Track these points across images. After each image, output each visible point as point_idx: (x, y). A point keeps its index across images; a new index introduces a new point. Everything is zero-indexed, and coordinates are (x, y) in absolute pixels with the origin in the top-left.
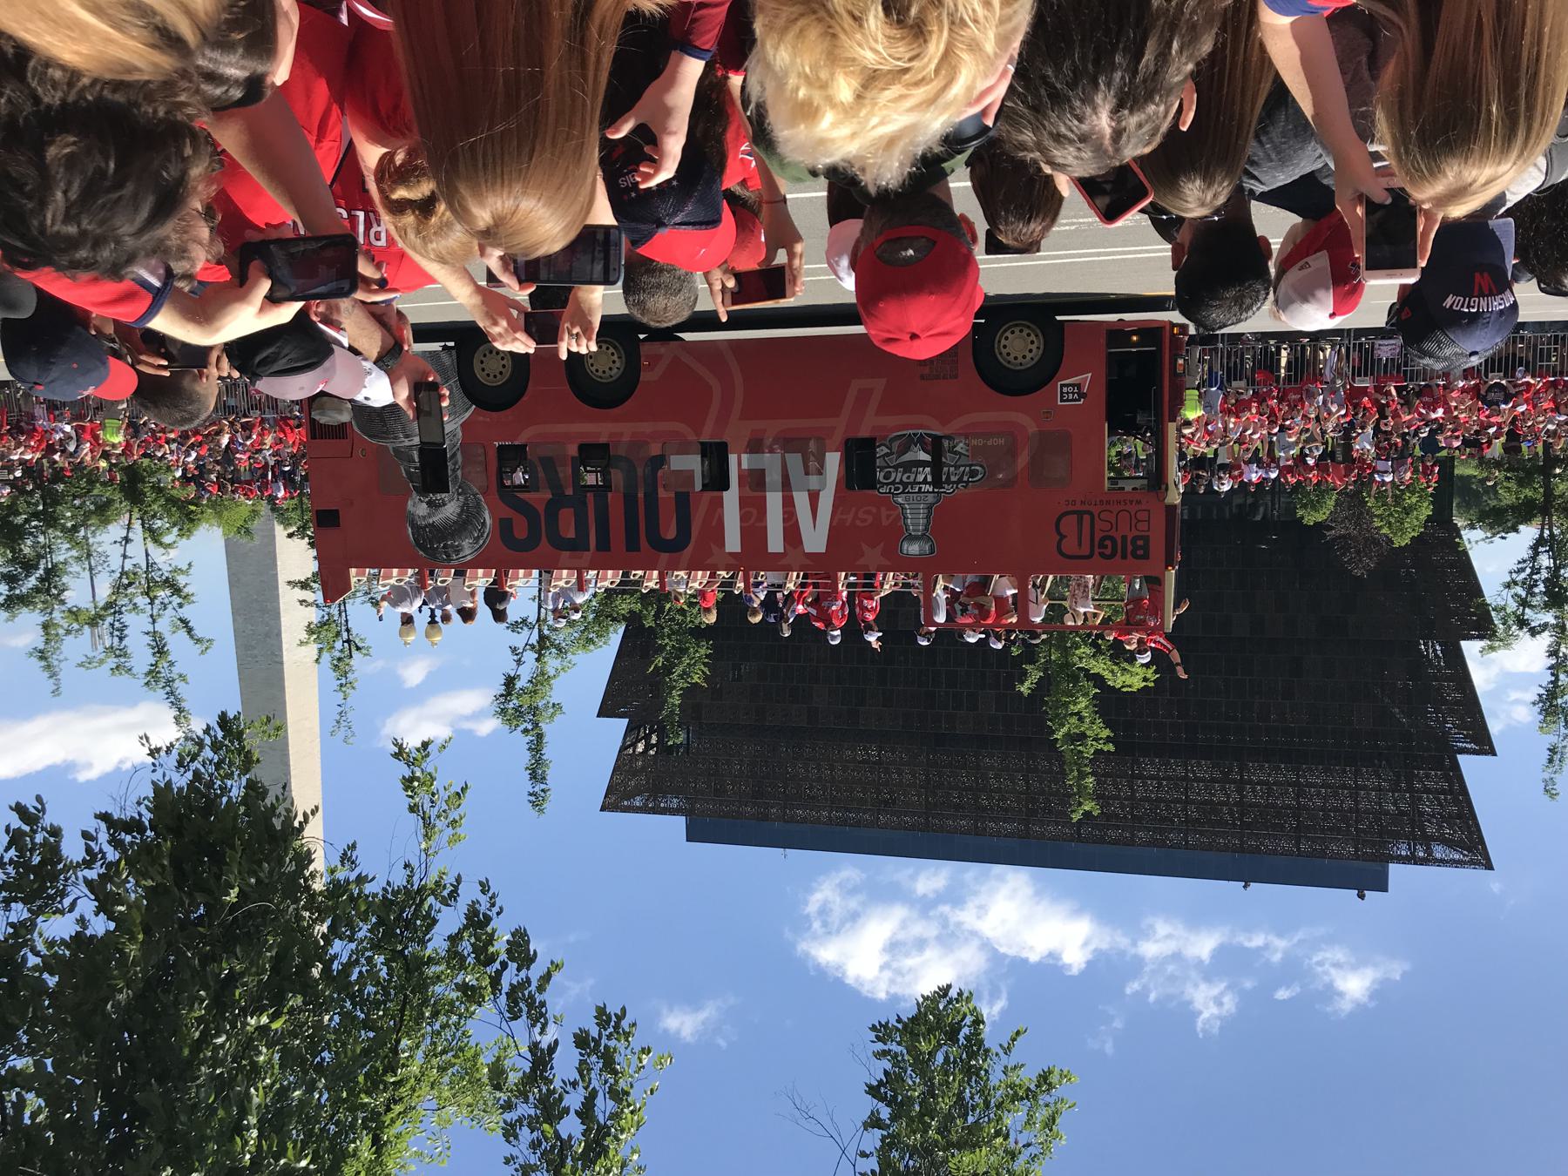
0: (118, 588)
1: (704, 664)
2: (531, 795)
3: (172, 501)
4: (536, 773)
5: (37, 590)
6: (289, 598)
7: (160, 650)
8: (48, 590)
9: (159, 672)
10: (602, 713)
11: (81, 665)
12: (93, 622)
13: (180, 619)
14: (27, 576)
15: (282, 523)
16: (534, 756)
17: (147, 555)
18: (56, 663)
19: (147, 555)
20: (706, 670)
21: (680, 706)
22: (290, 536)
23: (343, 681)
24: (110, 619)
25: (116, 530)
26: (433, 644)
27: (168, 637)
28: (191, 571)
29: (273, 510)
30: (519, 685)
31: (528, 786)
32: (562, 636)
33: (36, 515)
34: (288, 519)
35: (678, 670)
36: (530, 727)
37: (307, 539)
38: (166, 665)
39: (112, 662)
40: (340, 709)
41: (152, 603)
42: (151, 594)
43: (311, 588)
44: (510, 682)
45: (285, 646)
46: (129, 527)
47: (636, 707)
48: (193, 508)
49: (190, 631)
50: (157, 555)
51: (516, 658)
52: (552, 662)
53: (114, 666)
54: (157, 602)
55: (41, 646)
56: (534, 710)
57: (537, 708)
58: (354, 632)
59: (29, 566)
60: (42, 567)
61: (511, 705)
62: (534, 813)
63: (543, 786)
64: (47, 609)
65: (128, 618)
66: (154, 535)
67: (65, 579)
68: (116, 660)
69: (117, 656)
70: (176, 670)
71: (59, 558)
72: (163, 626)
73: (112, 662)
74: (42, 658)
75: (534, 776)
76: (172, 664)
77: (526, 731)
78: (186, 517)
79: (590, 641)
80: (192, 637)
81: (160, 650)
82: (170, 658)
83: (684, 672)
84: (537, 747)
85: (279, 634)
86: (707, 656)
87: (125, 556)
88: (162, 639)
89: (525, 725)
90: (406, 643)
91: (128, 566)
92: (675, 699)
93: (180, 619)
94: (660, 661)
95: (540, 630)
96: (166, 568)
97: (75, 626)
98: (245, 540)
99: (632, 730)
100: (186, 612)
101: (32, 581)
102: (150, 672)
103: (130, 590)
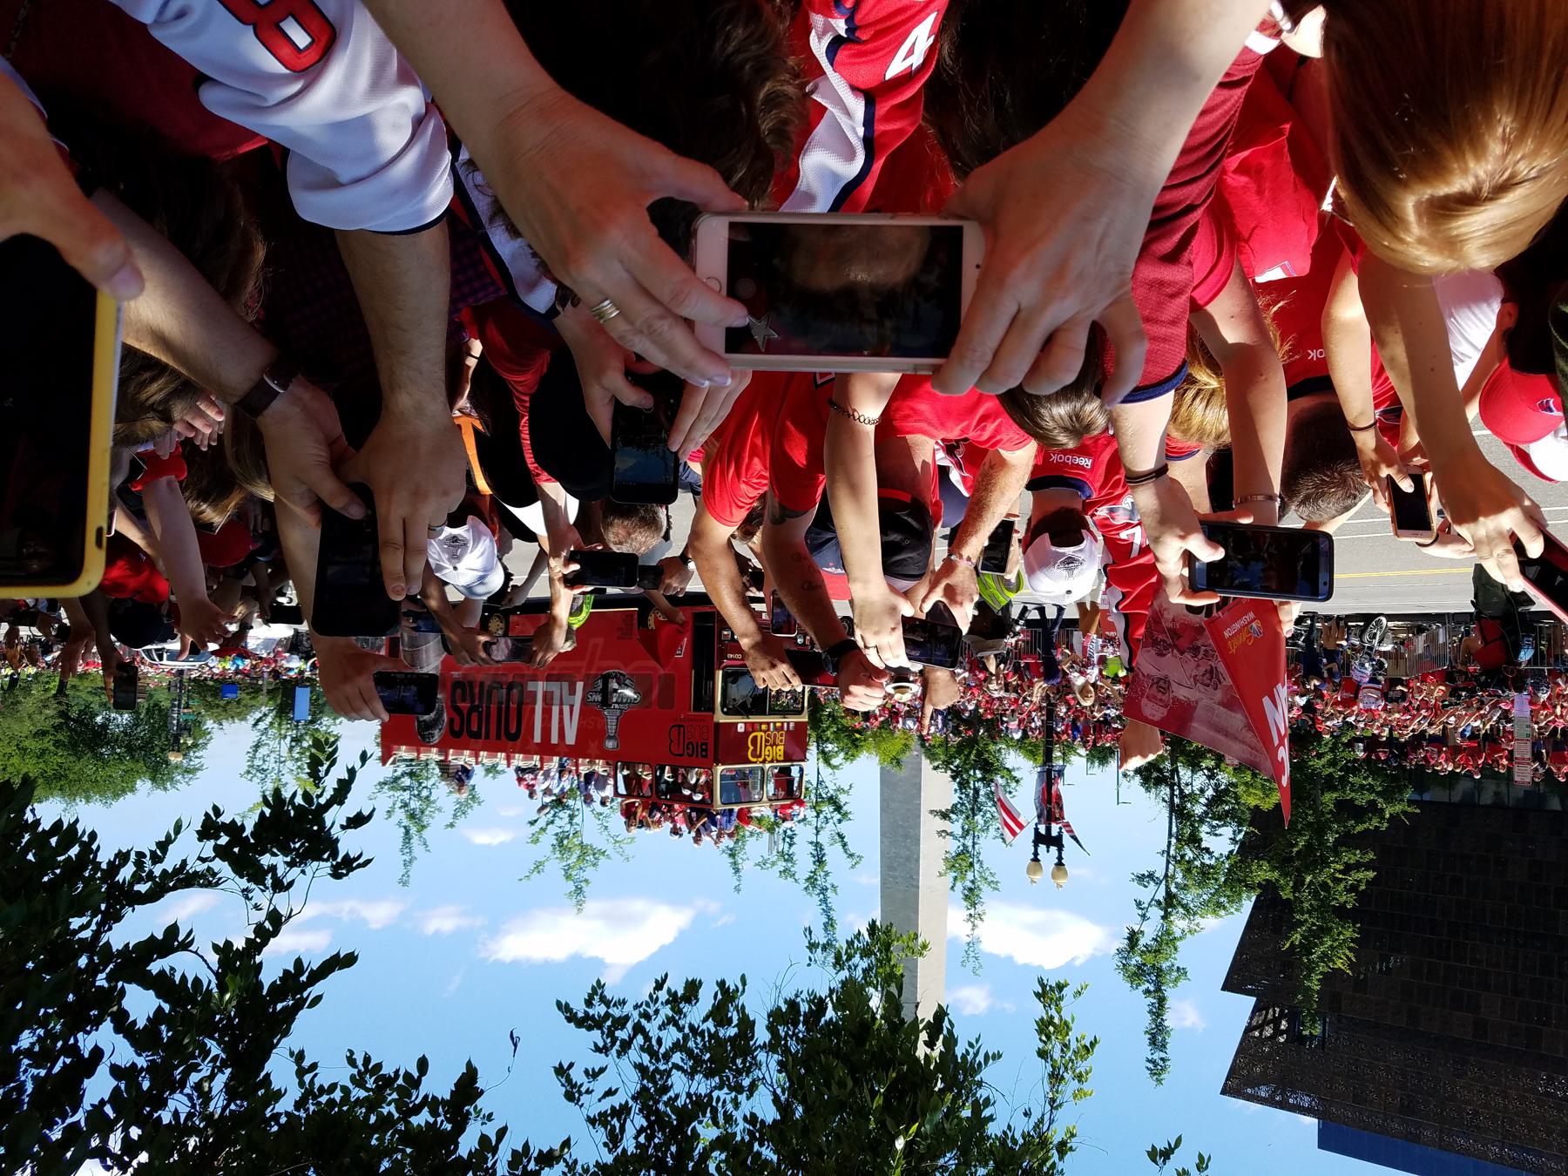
1: (1350, 949)
2: (1149, 1061)
3: (844, 729)
4: (1157, 1036)
6: (929, 826)
7: (820, 860)
9: (816, 880)
11: (758, 865)
13: (838, 834)
15: (929, 758)
17: (819, 773)
18: (740, 861)
19: (819, 773)
20: (1351, 955)
21: (1318, 992)
22: (936, 768)
23: (972, 911)
26: (1059, 886)
27: (827, 849)
30: (1143, 941)
31: (1146, 1050)
32: (1190, 897)
34: (933, 754)
35: (1318, 952)
36: (1152, 988)
37: (949, 772)
38: (822, 874)
39: (781, 865)
40: (968, 940)
41: (818, 817)
42: (818, 808)
43: (950, 818)
44: (1133, 938)
48: (858, 736)
49: (844, 845)
50: (826, 772)
51: (1140, 912)
52: (1179, 924)
53: (782, 869)
54: (821, 816)
56: (1159, 972)
57: (1160, 969)
58: (985, 867)
61: (1133, 962)
66: (826, 757)
68: (784, 864)
69: (785, 860)
72: (824, 838)
74: (732, 855)
75: (1153, 1041)
77: (1147, 992)
79: (1220, 905)
80: (846, 852)
81: (820, 860)
82: (825, 869)
83: (1324, 954)
85: (918, 860)
86: (1353, 940)
88: (822, 849)
90: (1033, 881)
92: (1314, 984)
93: (838, 834)
94: (1297, 937)
95: (1167, 887)
98: (895, 770)
100: (842, 828)
102: (808, 879)
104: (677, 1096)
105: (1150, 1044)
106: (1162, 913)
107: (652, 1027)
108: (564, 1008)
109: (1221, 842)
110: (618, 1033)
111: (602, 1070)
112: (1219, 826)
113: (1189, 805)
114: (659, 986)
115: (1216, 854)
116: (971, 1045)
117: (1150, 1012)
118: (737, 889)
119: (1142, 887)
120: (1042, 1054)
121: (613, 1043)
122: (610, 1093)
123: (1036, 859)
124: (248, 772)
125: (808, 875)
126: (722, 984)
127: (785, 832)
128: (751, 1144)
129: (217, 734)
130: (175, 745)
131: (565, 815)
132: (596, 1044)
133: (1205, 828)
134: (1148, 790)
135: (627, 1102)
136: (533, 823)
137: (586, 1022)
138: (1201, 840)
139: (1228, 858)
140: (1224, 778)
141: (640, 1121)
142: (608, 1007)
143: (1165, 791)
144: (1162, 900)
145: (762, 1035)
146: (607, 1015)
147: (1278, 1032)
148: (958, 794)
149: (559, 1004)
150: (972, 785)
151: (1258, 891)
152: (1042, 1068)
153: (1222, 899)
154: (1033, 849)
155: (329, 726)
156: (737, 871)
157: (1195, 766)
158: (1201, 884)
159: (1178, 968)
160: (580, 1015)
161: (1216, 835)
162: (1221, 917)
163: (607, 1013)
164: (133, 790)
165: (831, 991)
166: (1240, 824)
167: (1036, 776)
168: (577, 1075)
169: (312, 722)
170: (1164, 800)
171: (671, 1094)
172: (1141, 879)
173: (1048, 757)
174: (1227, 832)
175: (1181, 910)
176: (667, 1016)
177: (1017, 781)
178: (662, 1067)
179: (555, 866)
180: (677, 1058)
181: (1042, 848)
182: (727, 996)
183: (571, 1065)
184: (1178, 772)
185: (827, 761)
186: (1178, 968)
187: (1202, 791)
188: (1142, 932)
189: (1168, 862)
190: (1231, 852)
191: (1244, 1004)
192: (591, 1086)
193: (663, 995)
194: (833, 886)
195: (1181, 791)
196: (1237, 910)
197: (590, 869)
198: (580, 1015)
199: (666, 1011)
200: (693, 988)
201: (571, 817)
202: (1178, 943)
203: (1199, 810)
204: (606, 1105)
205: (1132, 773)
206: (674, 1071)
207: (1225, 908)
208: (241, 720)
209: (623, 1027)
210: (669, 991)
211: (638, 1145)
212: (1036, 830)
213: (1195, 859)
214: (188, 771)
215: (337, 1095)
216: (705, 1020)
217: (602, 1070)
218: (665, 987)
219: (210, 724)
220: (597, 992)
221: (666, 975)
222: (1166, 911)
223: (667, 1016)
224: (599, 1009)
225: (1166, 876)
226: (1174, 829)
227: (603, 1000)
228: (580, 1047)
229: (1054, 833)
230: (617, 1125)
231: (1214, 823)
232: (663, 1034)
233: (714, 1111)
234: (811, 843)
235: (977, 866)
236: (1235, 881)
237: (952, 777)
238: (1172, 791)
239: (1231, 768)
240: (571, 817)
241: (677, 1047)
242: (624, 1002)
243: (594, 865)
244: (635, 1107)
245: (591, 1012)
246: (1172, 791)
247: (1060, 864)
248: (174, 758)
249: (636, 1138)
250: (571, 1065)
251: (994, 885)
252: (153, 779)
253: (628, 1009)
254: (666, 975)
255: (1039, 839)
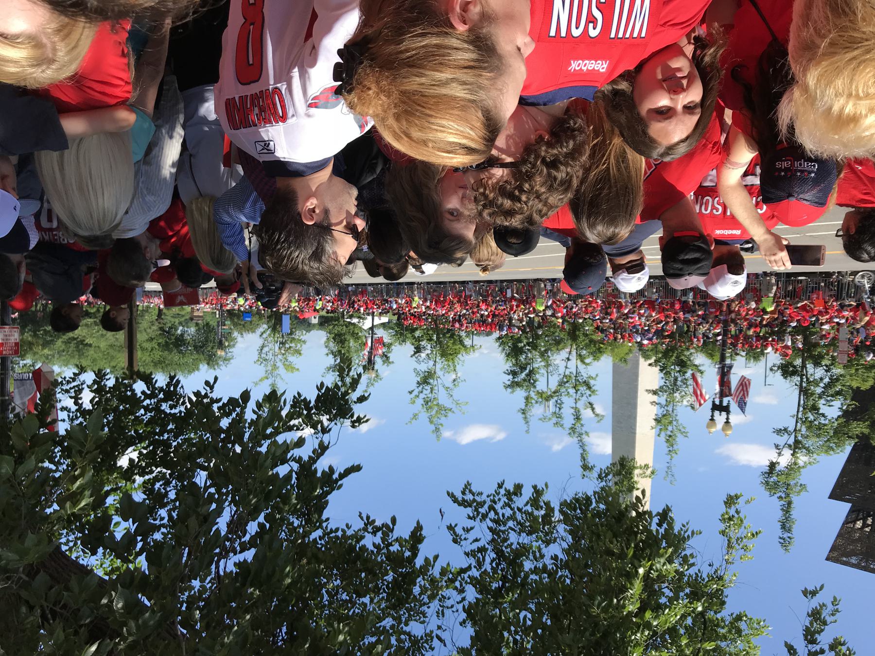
0: (561, 384)
2: (780, 538)
4: (786, 525)
5: (524, 380)
8: (529, 380)
10: (834, 495)
11: (540, 419)
12: (548, 399)
13: (589, 403)
14: (521, 372)
15: (644, 357)
16: (785, 515)
17: (577, 367)
18: (528, 417)
19: (577, 367)
22: (650, 365)
23: (671, 449)
24: (556, 398)
25: (564, 354)
26: (726, 435)
27: (582, 411)
28: (597, 379)
29: (640, 350)
30: (778, 468)
31: (779, 532)
32: (810, 443)
33: (528, 344)
34: (647, 355)
36: (783, 496)
37: (658, 368)
39: (554, 420)
40: (668, 465)
41: (576, 393)
45: (638, 424)
46: (570, 353)
47: (858, 497)
49: (593, 409)
51: (778, 451)
52: (802, 459)
54: (579, 392)
55: (523, 408)
57: (789, 485)
58: (680, 422)
59: (523, 368)
60: (528, 369)
62: (781, 550)
63: (789, 535)
64: (528, 390)
65: (564, 399)
66: (581, 358)
67: (537, 376)
70: (584, 429)
71: (536, 365)
72: (580, 405)
73: (554, 420)
74: (524, 413)
75: (783, 527)
76: (582, 425)
77: (780, 498)
78: (596, 348)
80: (594, 413)
81: (578, 418)
82: (582, 422)
84: (787, 508)
87: (566, 367)
89: (780, 494)
90: (710, 433)
91: (567, 373)
93: (589, 403)
95: (796, 437)
96: (585, 375)
97: (540, 400)
98: (623, 365)
99: (853, 511)
101: (523, 375)
102: (572, 428)
103: (567, 385)
104: (512, 544)
105: (782, 528)
106: (792, 452)
107: (498, 507)
108: (451, 495)
109: (832, 410)
110: (480, 510)
111: (472, 528)
112: (832, 401)
113: (812, 387)
114: (500, 486)
115: (829, 418)
116: (684, 526)
117: (782, 509)
118: (527, 431)
119: (779, 437)
120: (723, 533)
121: (478, 515)
122: (476, 540)
123: (712, 419)
124: (258, 360)
125: (571, 426)
126: (535, 487)
127: (557, 401)
128: (557, 572)
129: (239, 339)
130: (221, 345)
131: (428, 388)
132: (468, 515)
133: (822, 401)
134: (785, 378)
135: (484, 545)
136: (411, 393)
137: (464, 503)
138: (819, 408)
139: (837, 420)
140: (837, 371)
141: (493, 555)
142: (474, 496)
143: (797, 379)
144: (792, 444)
145: (557, 516)
146: (474, 500)
147: (865, 525)
148: (664, 380)
149: (448, 493)
150: (673, 375)
151: (857, 440)
152: (723, 541)
153: (831, 445)
154: (710, 414)
155: (300, 336)
156: (527, 422)
157: (817, 364)
158: (818, 436)
159: (801, 485)
160: (460, 499)
161: (829, 406)
162: (831, 455)
163: (474, 499)
164: (198, 369)
165: (595, 493)
166: (845, 399)
167: (716, 370)
168: (459, 530)
169: (291, 333)
170: (796, 385)
171: (509, 542)
172: (779, 432)
173: (723, 358)
174: (837, 403)
175: (804, 450)
176: (505, 502)
177: (702, 373)
178: (502, 528)
179: (424, 416)
180: (511, 524)
181: (717, 413)
182: (538, 492)
183: (456, 525)
184: (806, 368)
185: (583, 361)
186: (801, 485)
187: (821, 379)
188: (778, 463)
189: (797, 422)
190: (839, 417)
191: (844, 508)
192: (467, 536)
193: (502, 491)
194: (586, 432)
195: (808, 379)
196: (841, 451)
197: (443, 418)
198: (460, 499)
199: (505, 499)
200: (518, 488)
201: (432, 389)
202: (801, 470)
203: (819, 390)
204: (475, 546)
205: (776, 368)
206: (510, 530)
207: (833, 450)
208: (252, 332)
209: (482, 506)
210: (506, 489)
211: (492, 568)
212: (713, 402)
213: (815, 420)
214: (225, 359)
215: (340, 534)
216: (526, 505)
217: (472, 528)
218: (504, 486)
219: (236, 334)
220: (467, 488)
221: (504, 481)
222: (794, 452)
223: (505, 502)
224: (469, 497)
225: (795, 430)
226: (802, 402)
227: (471, 491)
228: (460, 516)
229: (725, 404)
230: (481, 557)
231: (829, 398)
232: (504, 511)
233: (534, 553)
234: (572, 408)
235: (674, 423)
236: (840, 433)
237: (660, 370)
238: (802, 379)
239: (841, 366)
240: (432, 389)
241: (513, 517)
242: (481, 494)
243: (446, 416)
244: (490, 548)
245: (465, 498)
246: (802, 379)
247: (727, 422)
248: (220, 353)
249: (491, 564)
250: (456, 525)
251: (685, 434)
252: (208, 364)
253: (484, 497)
254: (504, 481)
255: (715, 407)
